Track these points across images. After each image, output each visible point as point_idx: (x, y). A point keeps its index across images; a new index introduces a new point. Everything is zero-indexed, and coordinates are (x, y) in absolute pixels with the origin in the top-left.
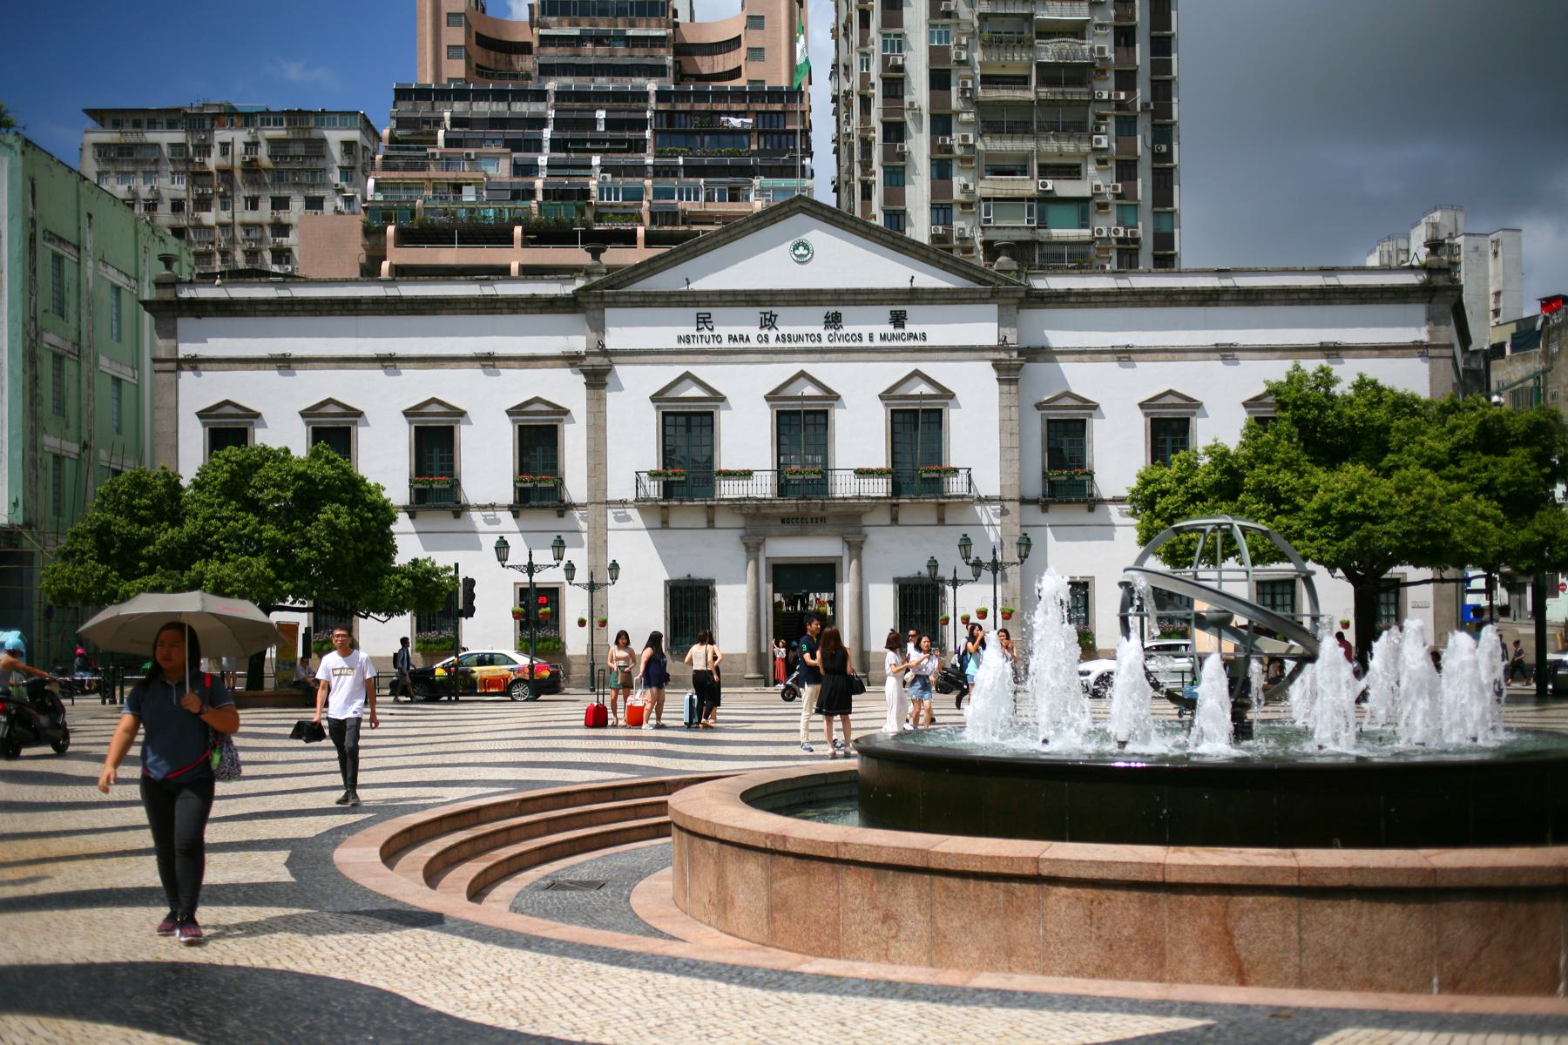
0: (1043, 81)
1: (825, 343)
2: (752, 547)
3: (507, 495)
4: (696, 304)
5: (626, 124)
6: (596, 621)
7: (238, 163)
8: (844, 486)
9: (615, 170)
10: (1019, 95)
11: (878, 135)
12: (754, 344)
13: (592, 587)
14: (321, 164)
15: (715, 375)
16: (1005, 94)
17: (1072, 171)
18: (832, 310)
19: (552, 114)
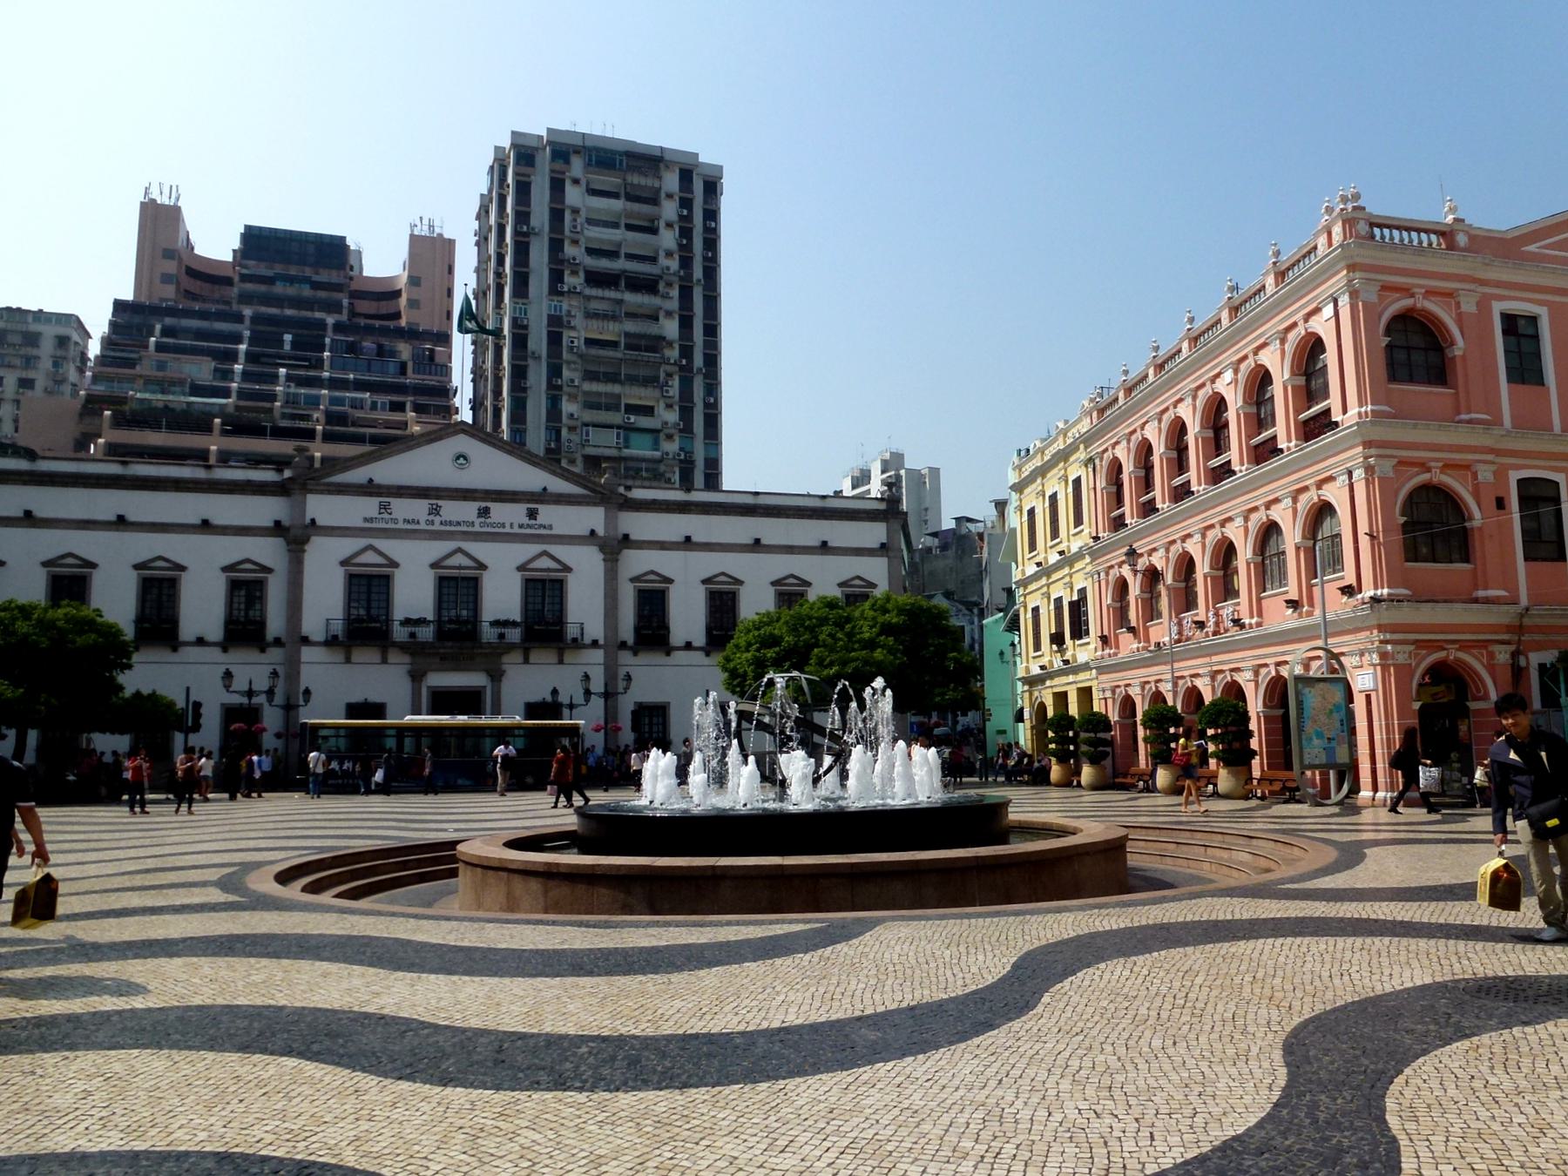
0: (629, 347)
1: (477, 528)
2: (416, 676)
8: (488, 634)
10: (610, 353)
12: (423, 526)
14: (34, 352)
15: (392, 547)
16: (602, 352)
17: (648, 411)
18: (484, 504)
19: (247, 333)
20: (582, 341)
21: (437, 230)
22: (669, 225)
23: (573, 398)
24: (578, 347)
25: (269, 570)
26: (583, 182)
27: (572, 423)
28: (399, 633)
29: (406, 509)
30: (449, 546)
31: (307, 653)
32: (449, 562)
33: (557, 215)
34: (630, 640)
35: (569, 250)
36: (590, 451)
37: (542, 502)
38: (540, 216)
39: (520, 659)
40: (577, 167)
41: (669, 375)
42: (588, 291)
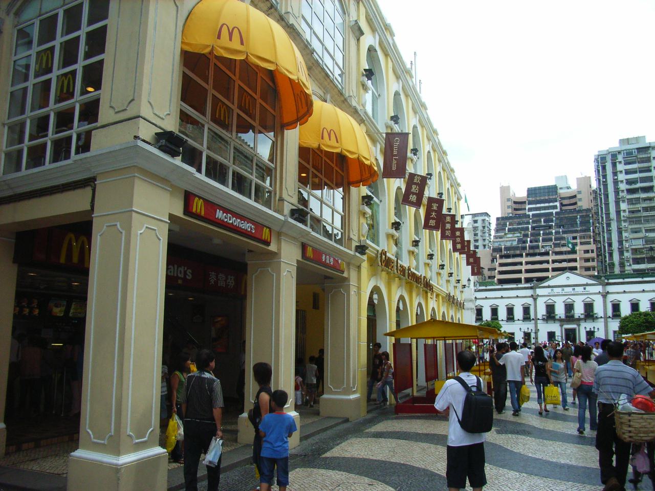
1: (572, 293)
2: (561, 326)
6: (536, 338)
8: (576, 316)
12: (561, 294)
13: (535, 333)
15: (554, 298)
26: (623, 162)
27: (627, 239)
28: (557, 317)
29: (557, 290)
30: (566, 297)
34: (611, 316)
40: (620, 158)
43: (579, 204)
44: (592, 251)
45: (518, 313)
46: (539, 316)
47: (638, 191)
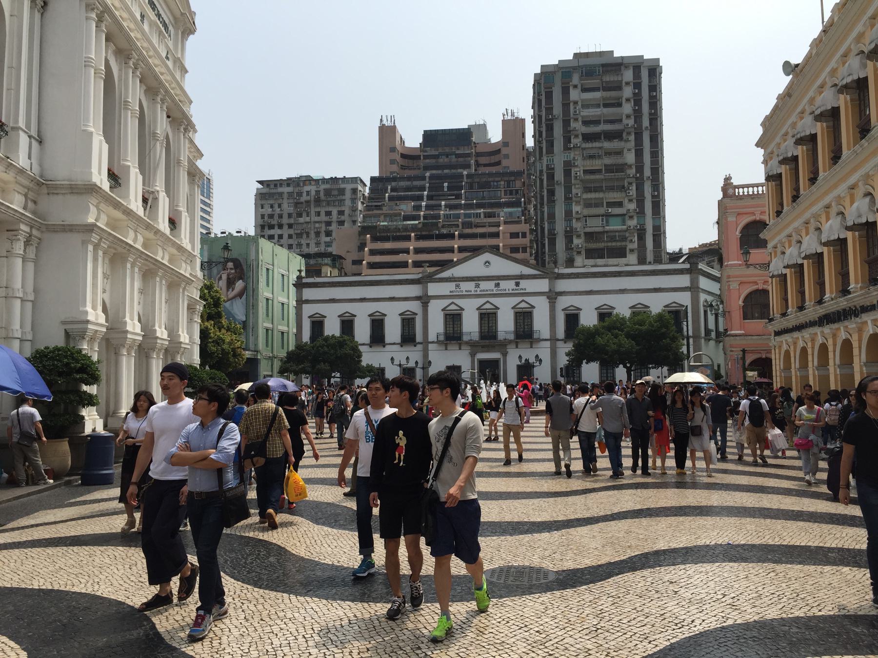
1: (495, 292)
2: (473, 355)
3: (399, 340)
4: (456, 281)
5: (455, 188)
7: (312, 199)
8: (501, 336)
9: (450, 207)
10: (597, 177)
11: (545, 193)
12: (473, 293)
13: (423, 368)
14: (344, 198)
15: (461, 302)
16: (592, 177)
17: (620, 204)
18: (497, 282)
19: (428, 185)
20: (582, 171)
21: (516, 115)
22: (628, 100)
23: (578, 203)
24: (579, 176)
25: (416, 314)
26: (579, 86)
27: (579, 216)
28: (465, 338)
29: (467, 286)
30: (484, 300)
31: (431, 346)
32: (485, 307)
33: (566, 105)
35: (573, 125)
36: (588, 230)
37: (521, 279)
38: (557, 110)
39: (514, 346)
40: (576, 79)
41: (630, 184)
42: (584, 145)
43: (505, 163)
44: (524, 235)
45: (393, 331)
46: (432, 337)
47: (600, 138)
